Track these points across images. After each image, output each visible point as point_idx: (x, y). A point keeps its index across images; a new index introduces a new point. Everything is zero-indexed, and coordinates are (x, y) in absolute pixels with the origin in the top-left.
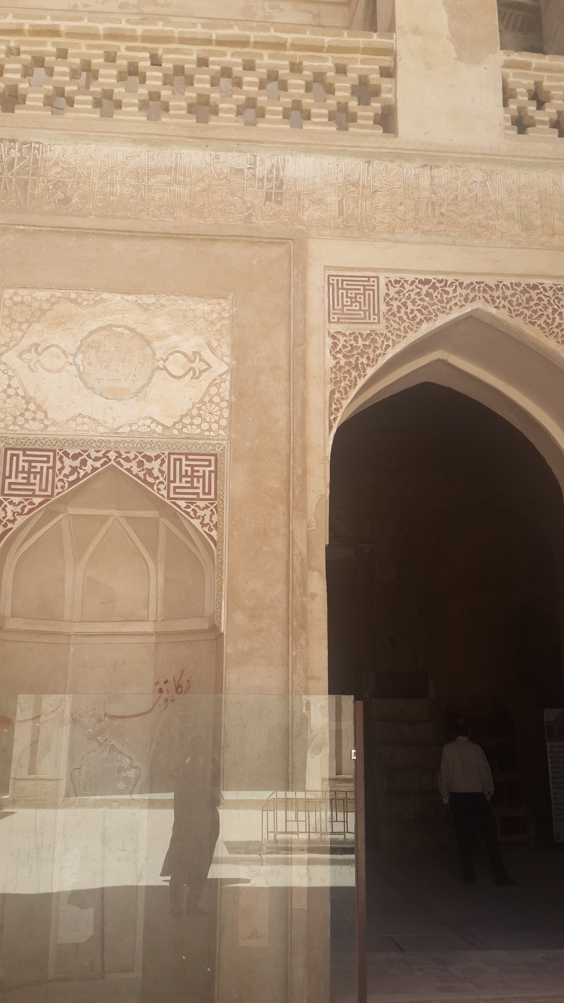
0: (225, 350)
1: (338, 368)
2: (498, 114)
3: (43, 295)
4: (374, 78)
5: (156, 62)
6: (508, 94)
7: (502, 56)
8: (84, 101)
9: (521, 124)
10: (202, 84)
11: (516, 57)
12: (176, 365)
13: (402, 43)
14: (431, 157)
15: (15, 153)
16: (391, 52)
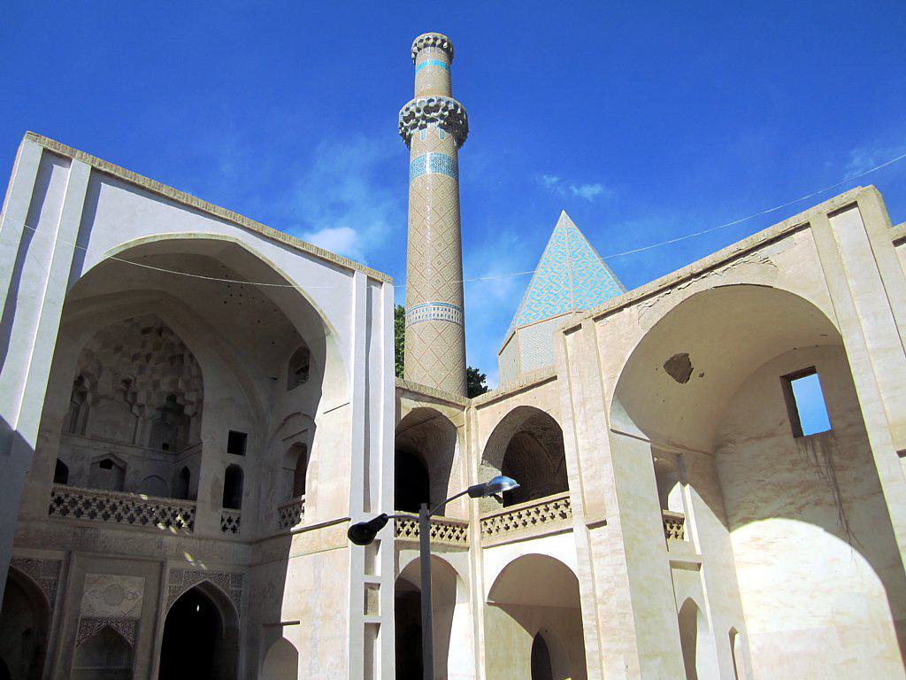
0: (142, 592)
1: (170, 596)
2: (219, 526)
3: (96, 575)
4: (189, 513)
5: (133, 504)
6: (223, 520)
7: (222, 509)
8: (113, 517)
9: (224, 528)
10: (145, 513)
11: (226, 510)
12: (130, 596)
13: (199, 505)
14: (200, 539)
15: (92, 532)
16: (195, 507)
